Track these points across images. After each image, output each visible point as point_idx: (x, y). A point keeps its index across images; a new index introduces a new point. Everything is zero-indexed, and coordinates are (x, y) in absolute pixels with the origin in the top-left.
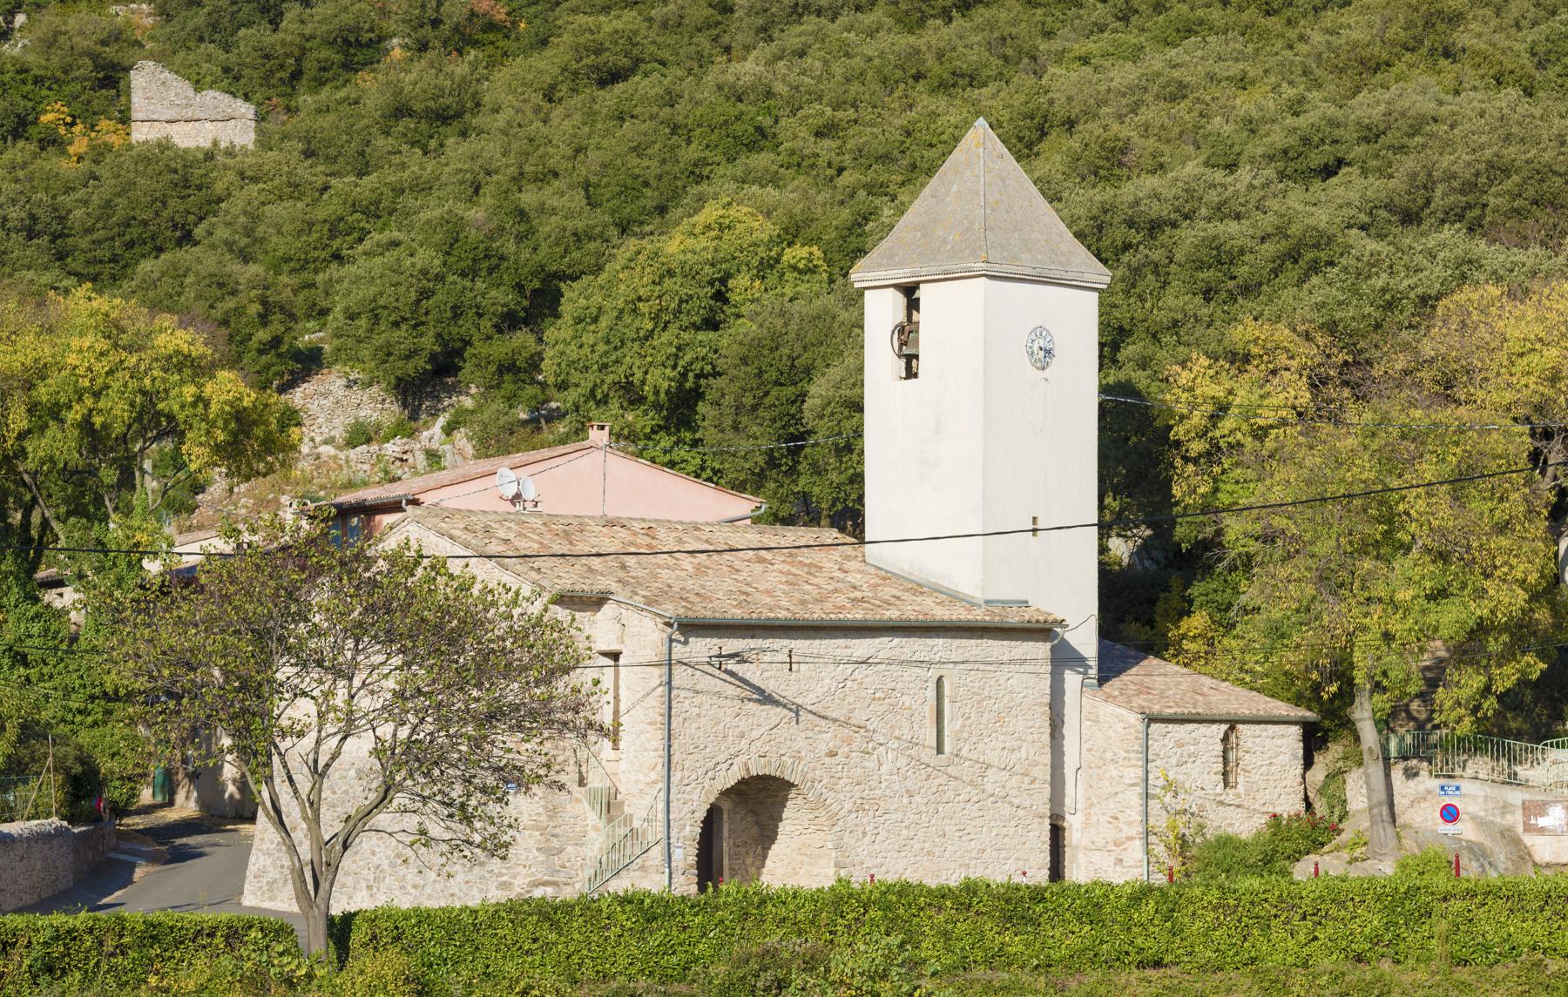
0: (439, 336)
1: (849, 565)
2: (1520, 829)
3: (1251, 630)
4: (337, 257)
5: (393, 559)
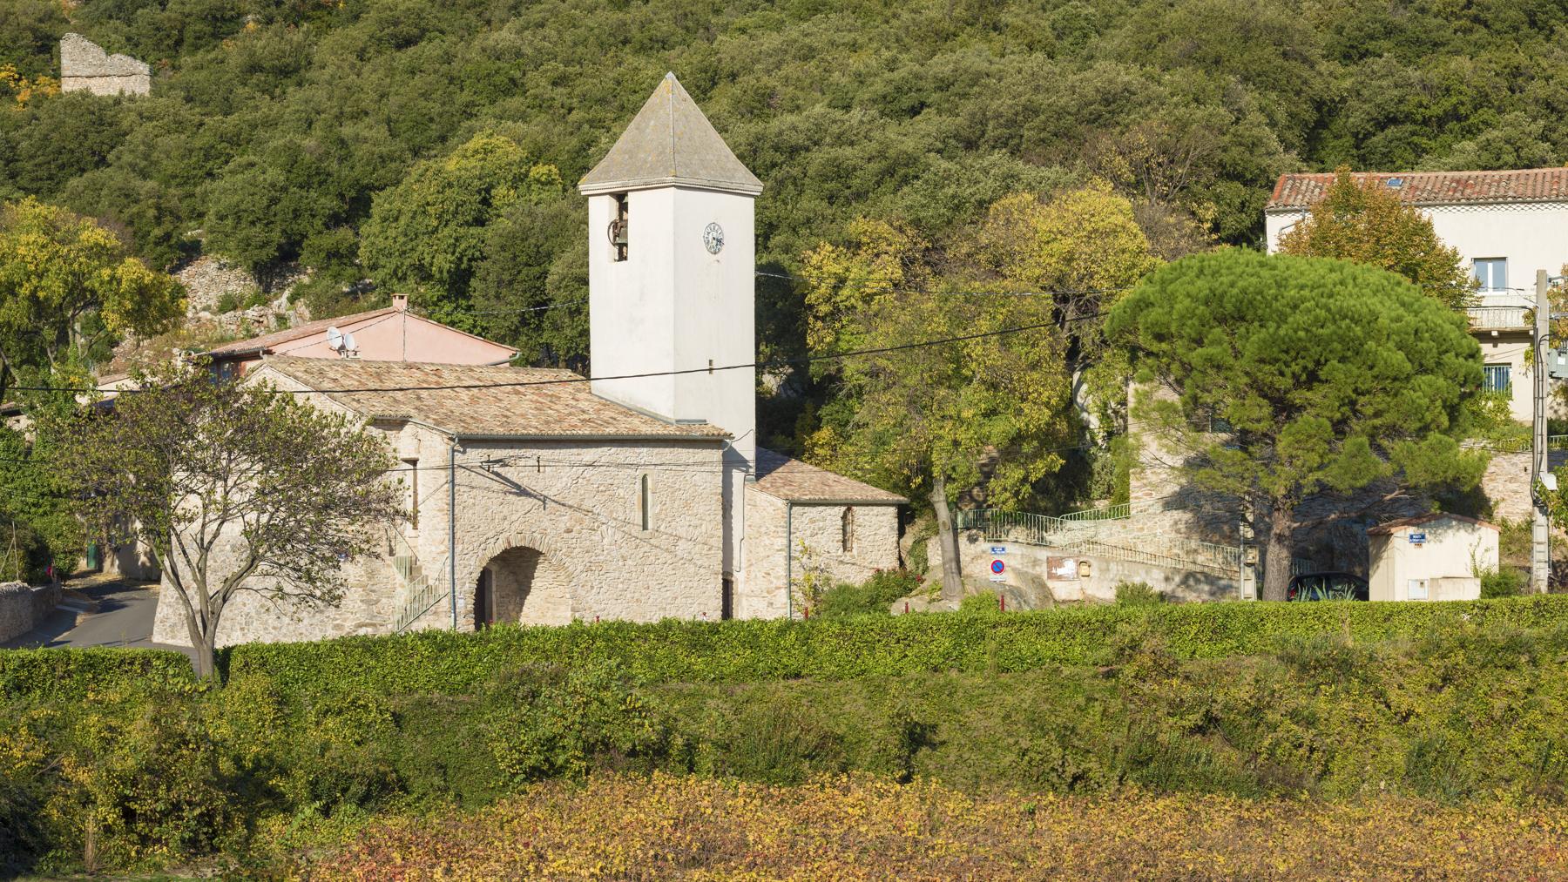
0: (284, 231)
1: (579, 395)
2: (1045, 577)
3: (862, 440)
4: (210, 174)
5: (255, 394)
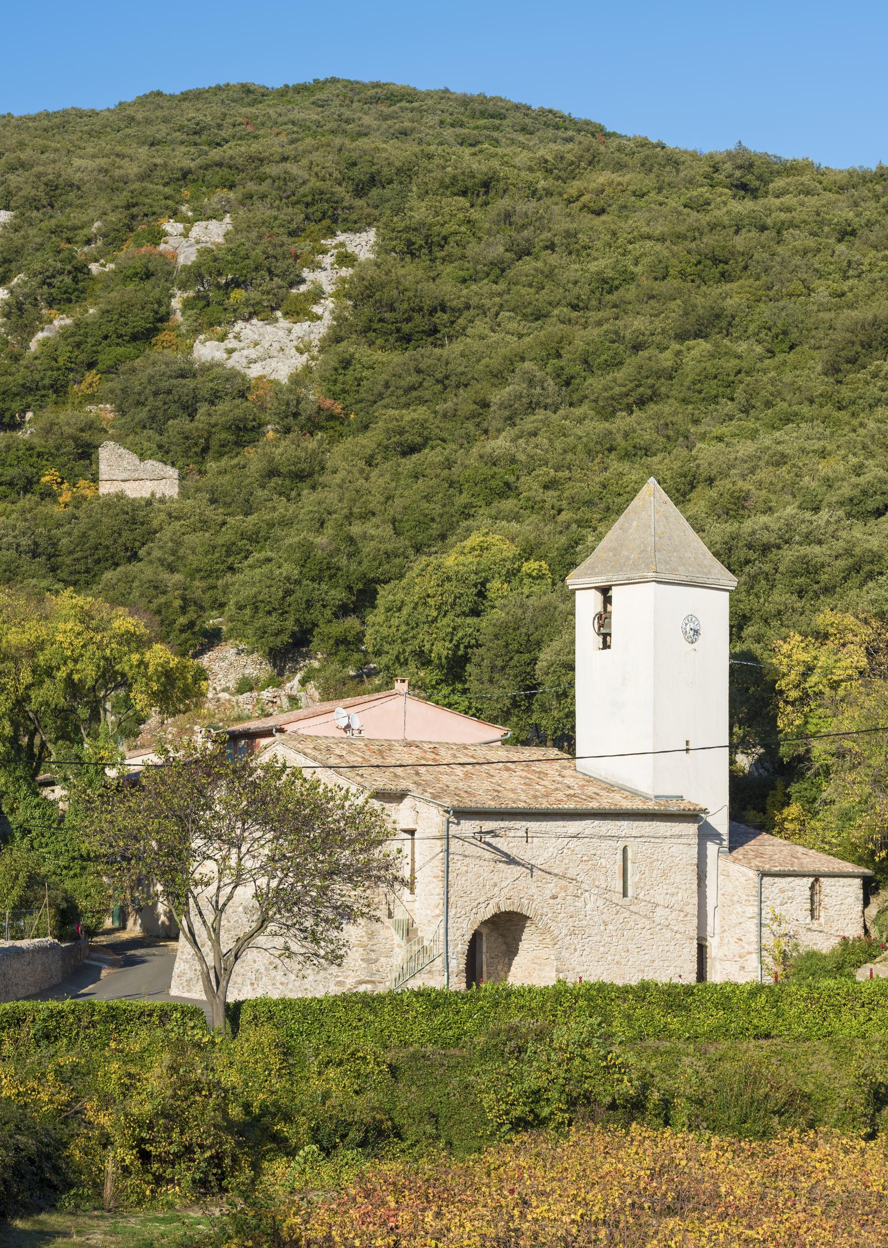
0: (297, 620)
3: (829, 816)
4: (231, 569)
5: (267, 768)
